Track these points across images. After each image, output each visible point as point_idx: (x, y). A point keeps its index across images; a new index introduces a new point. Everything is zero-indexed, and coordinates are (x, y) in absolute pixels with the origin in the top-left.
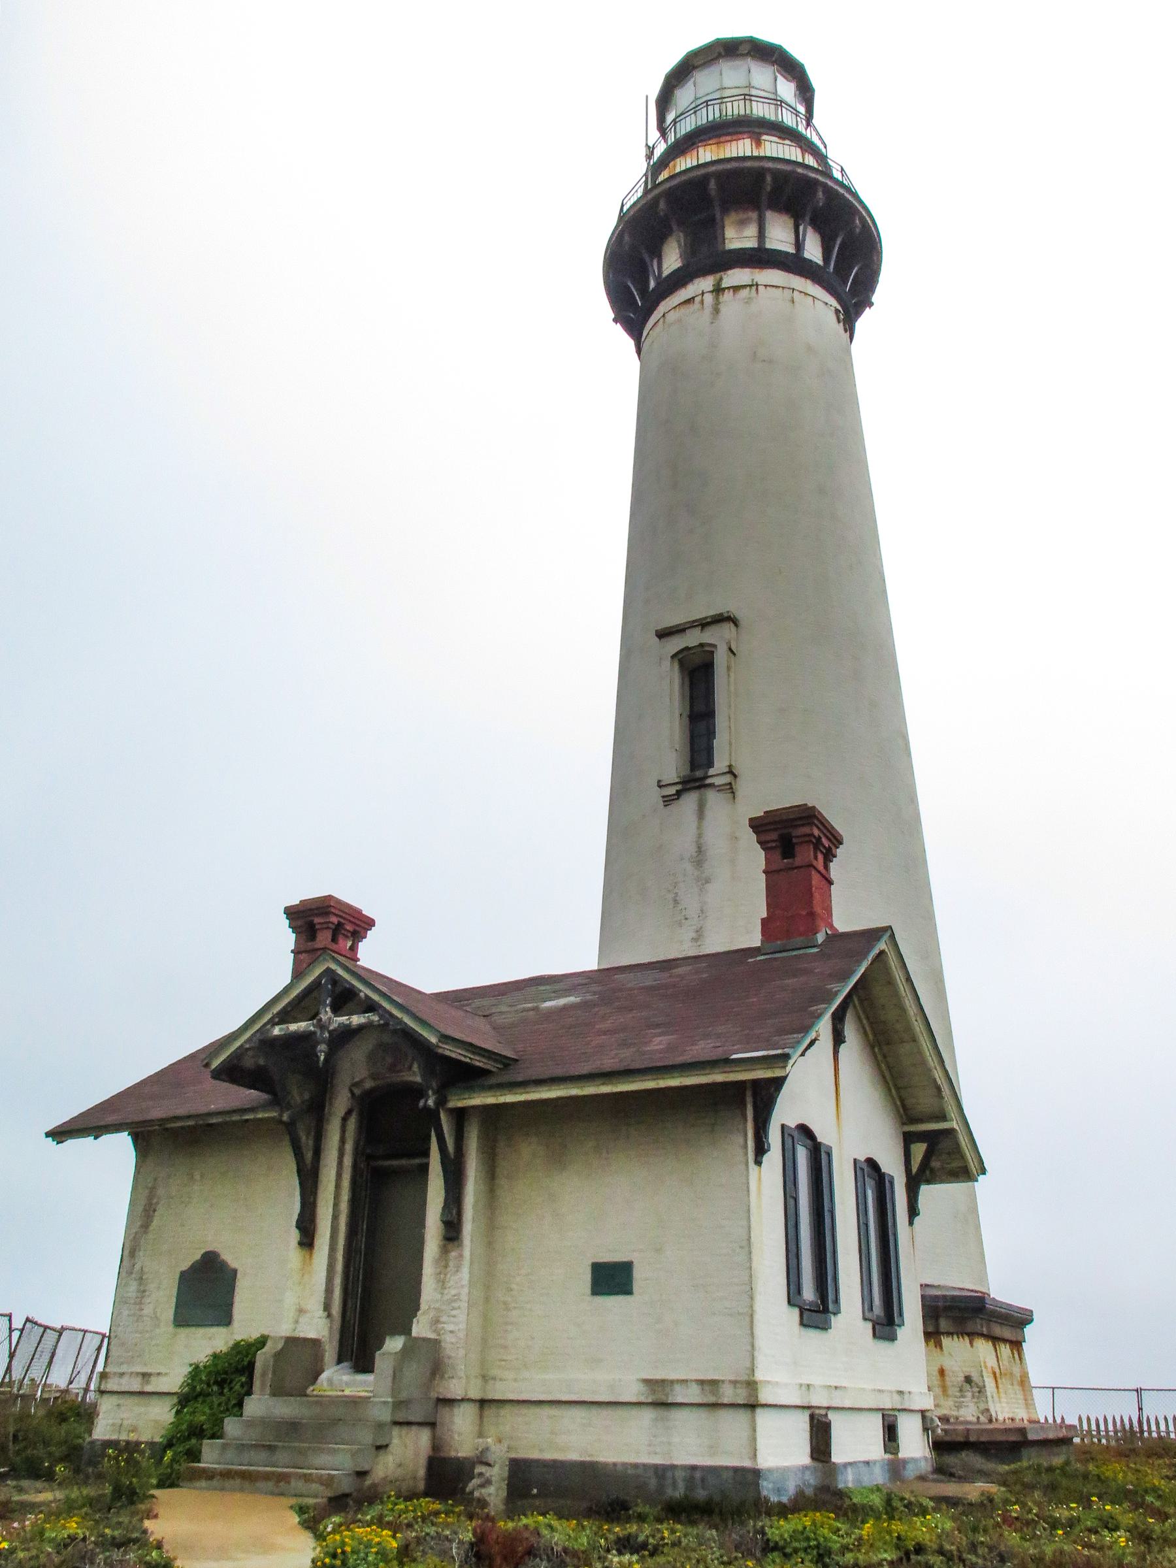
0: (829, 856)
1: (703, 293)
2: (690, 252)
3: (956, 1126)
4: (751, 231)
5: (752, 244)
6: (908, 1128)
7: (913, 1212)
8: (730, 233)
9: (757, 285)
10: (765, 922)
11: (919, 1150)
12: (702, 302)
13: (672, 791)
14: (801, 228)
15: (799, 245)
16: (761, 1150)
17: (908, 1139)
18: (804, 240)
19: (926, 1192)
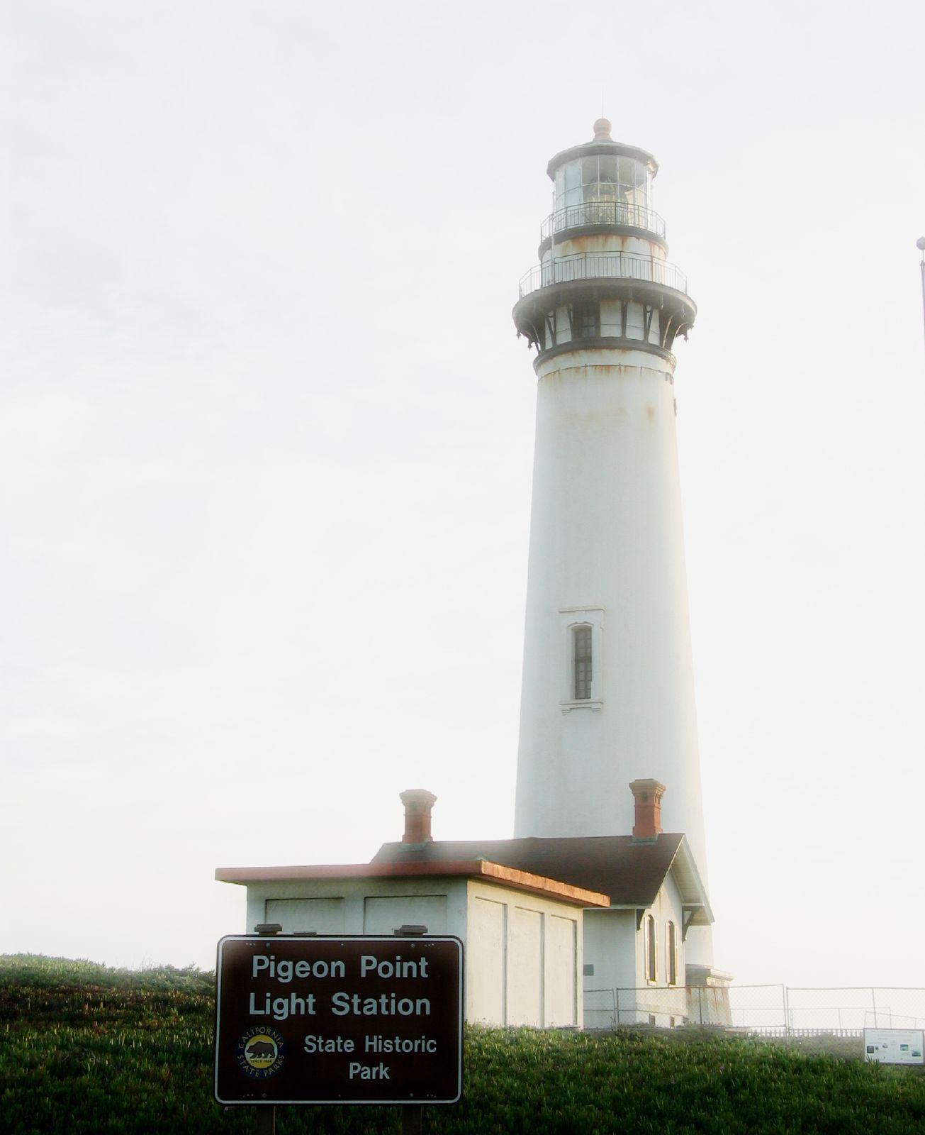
0: (659, 798)
1: (586, 366)
2: (577, 327)
3: (704, 905)
4: (617, 319)
5: (615, 332)
6: (687, 905)
7: (683, 939)
8: (604, 318)
9: (620, 366)
10: (634, 828)
11: (688, 914)
12: (586, 371)
13: (568, 708)
14: (648, 314)
15: (646, 331)
16: (638, 928)
17: (684, 909)
18: (649, 326)
19: (690, 928)
